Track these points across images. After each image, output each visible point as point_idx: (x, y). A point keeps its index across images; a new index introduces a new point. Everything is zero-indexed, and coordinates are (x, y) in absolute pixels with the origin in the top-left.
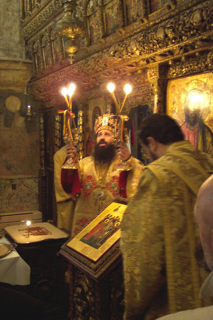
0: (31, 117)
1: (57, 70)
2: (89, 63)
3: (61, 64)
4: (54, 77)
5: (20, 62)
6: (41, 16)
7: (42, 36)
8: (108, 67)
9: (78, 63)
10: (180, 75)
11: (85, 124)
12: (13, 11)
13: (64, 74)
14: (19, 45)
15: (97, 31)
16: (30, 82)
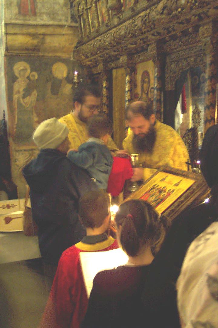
0: (78, 83)
1: (103, 33)
2: (136, 23)
3: (107, 25)
5: (64, 26)
9: (125, 24)
11: (133, 88)
13: (110, 36)
14: (64, 8)
16: (76, 47)
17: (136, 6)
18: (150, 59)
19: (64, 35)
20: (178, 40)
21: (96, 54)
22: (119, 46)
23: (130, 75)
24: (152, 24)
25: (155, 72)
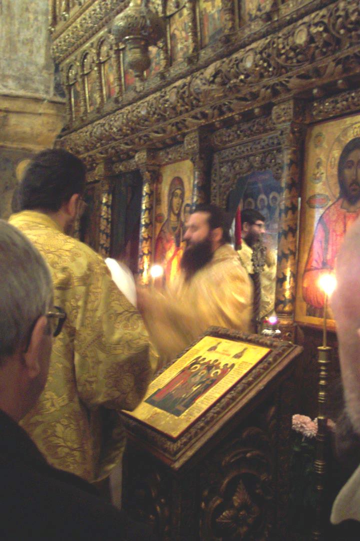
1: (109, 114)
2: (167, 97)
3: (116, 101)
4: (103, 125)
5: (43, 100)
6: (85, 19)
7: (85, 56)
8: (201, 104)
9: (147, 99)
10: (331, 116)
11: (154, 206)
12: (36, 12)
13: (121, 119)
14: (44, 71)
15: (183, 41)
16: (60, 136)
17: (168, 71)
18: (187, 159)
19: (40, 114)
20: (234, 129)
21: (95, 147)
22: (135, 136)
23: (149, 184)
24: (195, 98)
25: (194, 177)
